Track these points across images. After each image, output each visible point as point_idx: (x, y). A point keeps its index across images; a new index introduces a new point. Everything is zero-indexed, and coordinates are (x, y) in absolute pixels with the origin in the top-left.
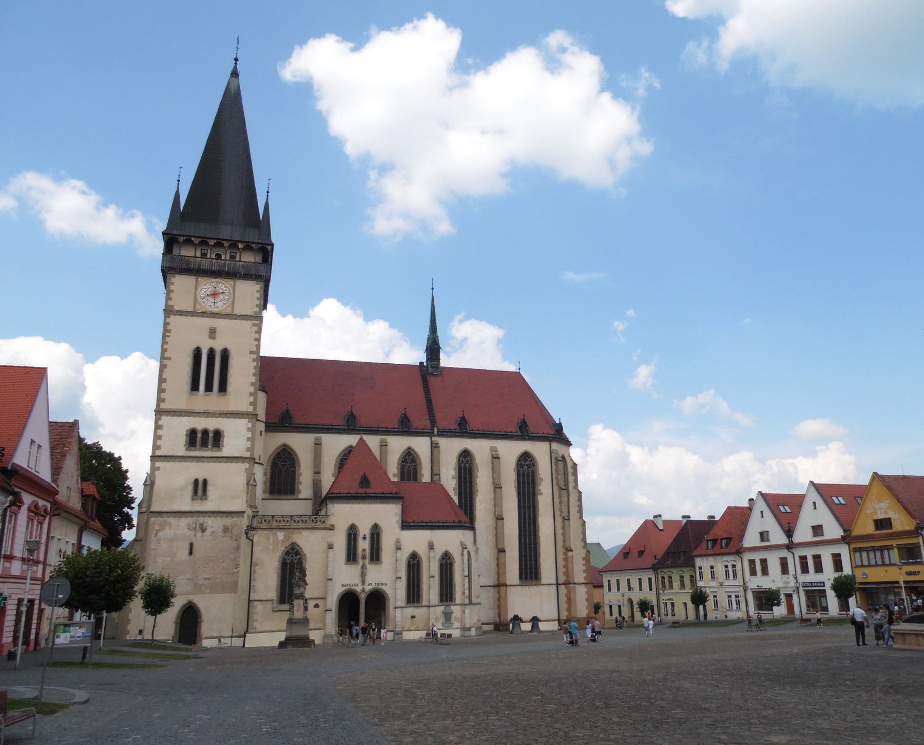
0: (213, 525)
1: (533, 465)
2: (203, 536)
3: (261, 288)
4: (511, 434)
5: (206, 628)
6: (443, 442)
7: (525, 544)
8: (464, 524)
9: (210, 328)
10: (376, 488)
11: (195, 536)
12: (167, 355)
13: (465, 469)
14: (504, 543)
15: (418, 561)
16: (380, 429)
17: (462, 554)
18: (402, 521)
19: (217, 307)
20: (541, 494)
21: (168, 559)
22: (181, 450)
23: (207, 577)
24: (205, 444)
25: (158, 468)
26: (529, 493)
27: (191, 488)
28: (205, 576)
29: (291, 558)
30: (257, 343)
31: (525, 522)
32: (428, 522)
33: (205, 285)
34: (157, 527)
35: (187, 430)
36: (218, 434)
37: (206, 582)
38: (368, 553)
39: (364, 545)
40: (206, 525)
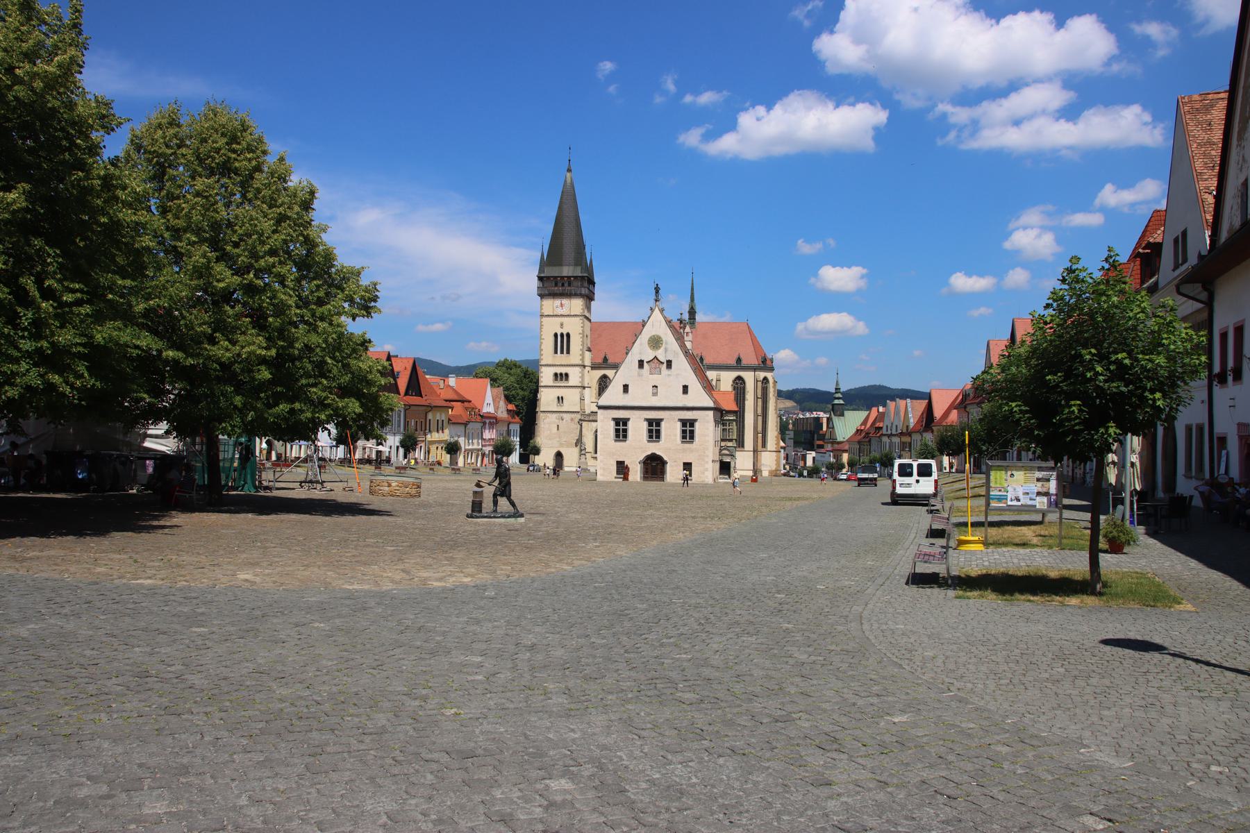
5: (566, 462)
22: (551, 383)
24: (561, 380)
27: (556, 400)
36: (567, 375)
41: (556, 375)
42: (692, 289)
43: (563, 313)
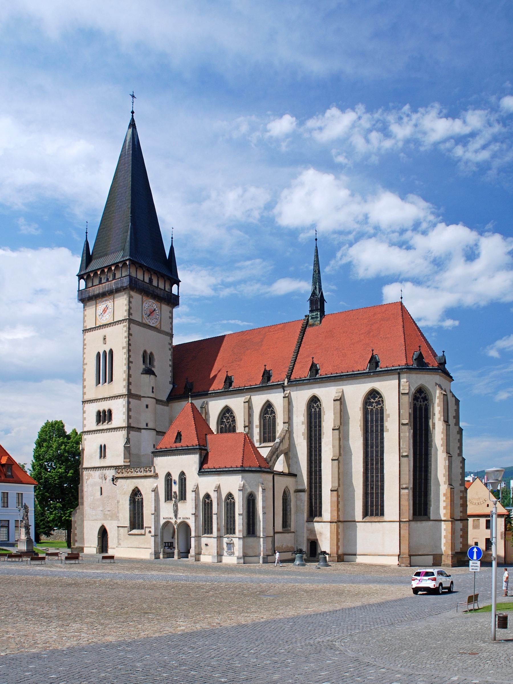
1: (383, 401)
2: (105, 483)
10: (184, 443)
11: (102, 483)
12: (85, 362)
15: (211, 501)
16: (245, 388)
21: (92, 497)
23: (109, 509)
26: (377, 431)
27: (99, 451)
32: (219, 468)
36: (110, 411)
37: (109, 513)
39: (175, 488)
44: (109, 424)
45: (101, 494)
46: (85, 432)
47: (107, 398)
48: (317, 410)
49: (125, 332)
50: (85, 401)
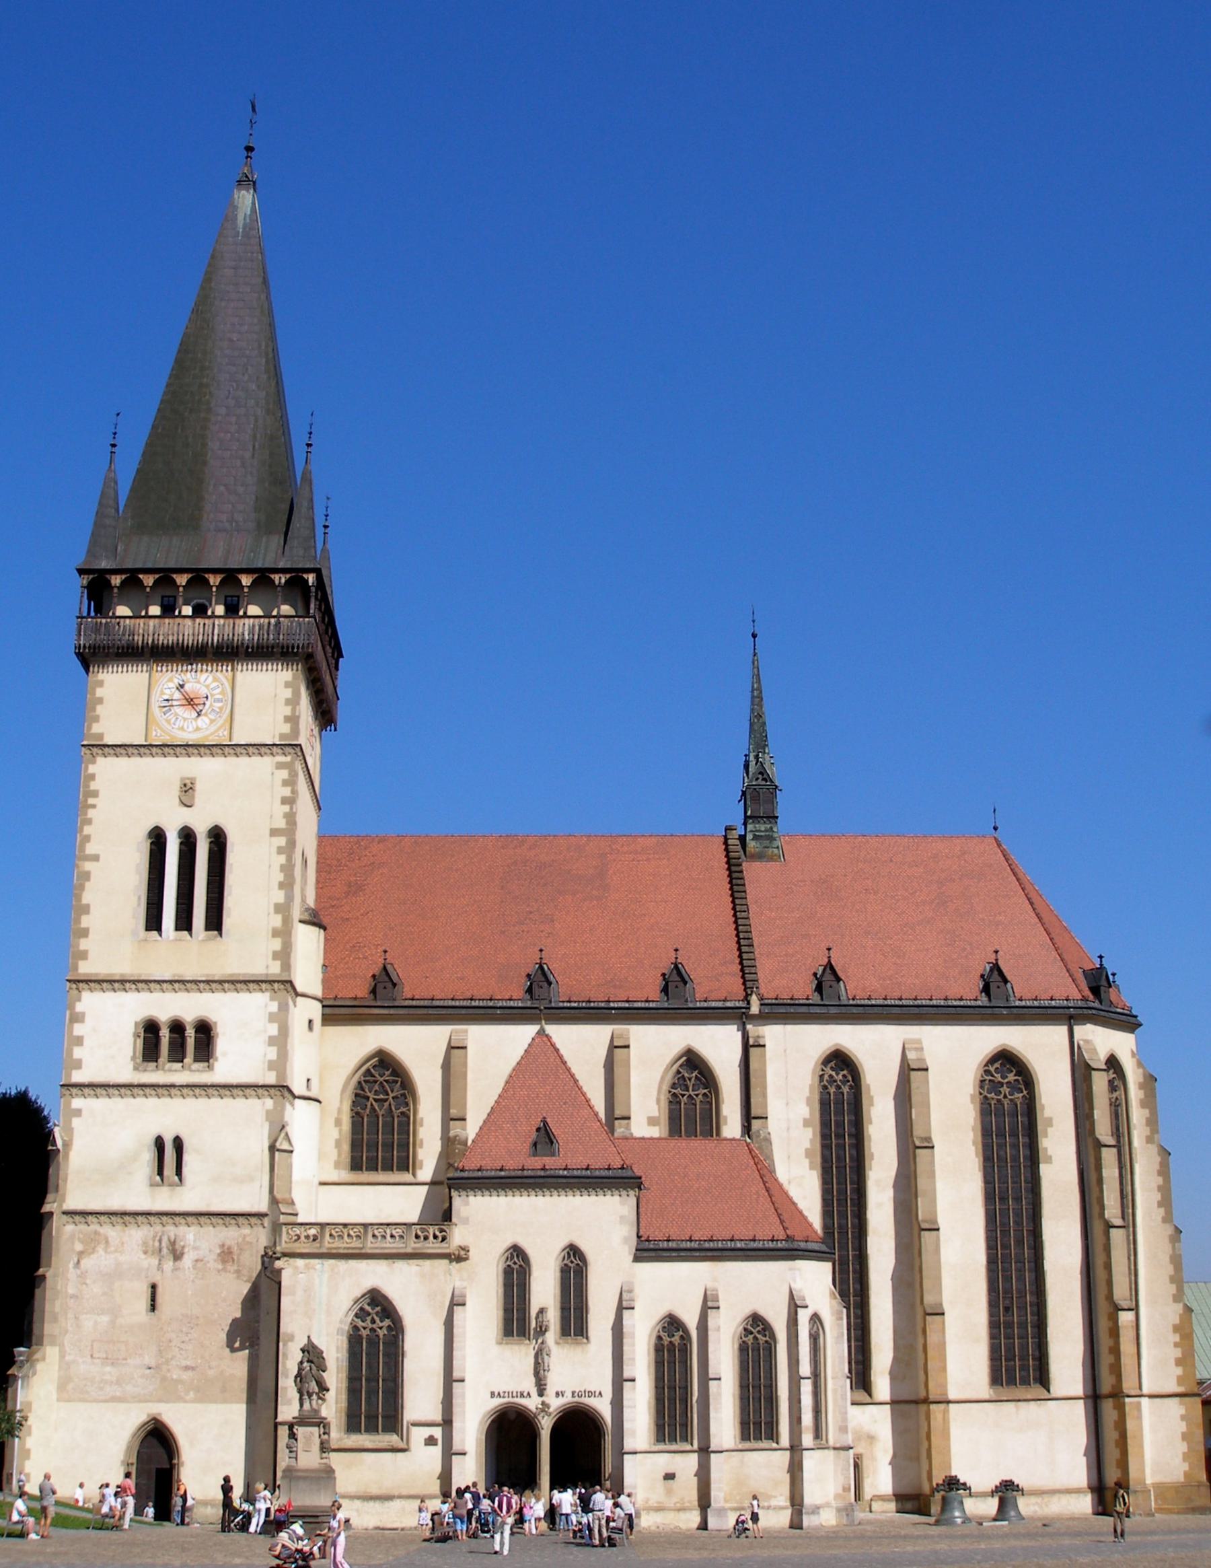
0: (198, 1244)
3: (294, 677)
4: (962, 1003)
6: (773, 1035)
7: (1007, 1291)
8: (803, 1245)
9: (182, 779)
10: (570, 1156)
13: (840, 1102)
14: (940, 1293)
16: (612, 1005)
17: (793, 1322)
18: (639, 1237)
19: (198, 729)
20: (1049, 1160)
21: (105, 1319)
22: (126, 1074)
23: (188, 1363)
24: (177, 1054)
25: (78, 1113)
27: (148, 1156)
28: (184, 1363)
29: (370, 1326)
30: (286, 808)
31: (1005, 1233)
33: (171, 680)
34: (79, 1247)
35: (136, 1023)
36: (205, 1030)
37: (186, 1376)
38: (553, 1317)
40: (182, 1243)
41: (151, 1028)
42: (757, 698)
43: (191, 737)
44: (198, 1071)
45: (153, 1307)
46: (80, 1086)
47: (196, 982)
48: (846, 1089)
49: (285, 783)
50: (87, 982)
